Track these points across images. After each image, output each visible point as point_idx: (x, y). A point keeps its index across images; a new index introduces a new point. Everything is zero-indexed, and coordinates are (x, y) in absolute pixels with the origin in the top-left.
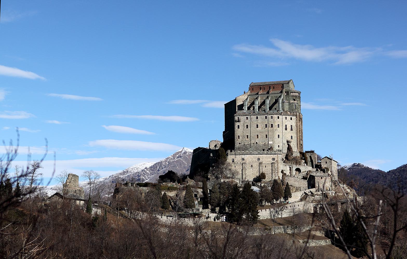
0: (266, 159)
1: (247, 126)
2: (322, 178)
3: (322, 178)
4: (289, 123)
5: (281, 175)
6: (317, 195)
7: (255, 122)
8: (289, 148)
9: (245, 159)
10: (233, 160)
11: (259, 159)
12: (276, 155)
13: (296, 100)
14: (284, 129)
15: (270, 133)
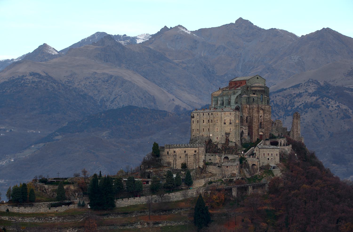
0: (191, 151)
1: (198, 121)
2: (227, 167)
3: (227, 167)
4: (228, 117)
5: (201, 164)
6: (215, 182)
7: (202, 118)
8: (227, 140)
9: (176, 151)
10: (168, 152)
11: (185, 152)
12: (198, 148)
13: (256, 94)
14: (223, 123)
15: (211, 127)
